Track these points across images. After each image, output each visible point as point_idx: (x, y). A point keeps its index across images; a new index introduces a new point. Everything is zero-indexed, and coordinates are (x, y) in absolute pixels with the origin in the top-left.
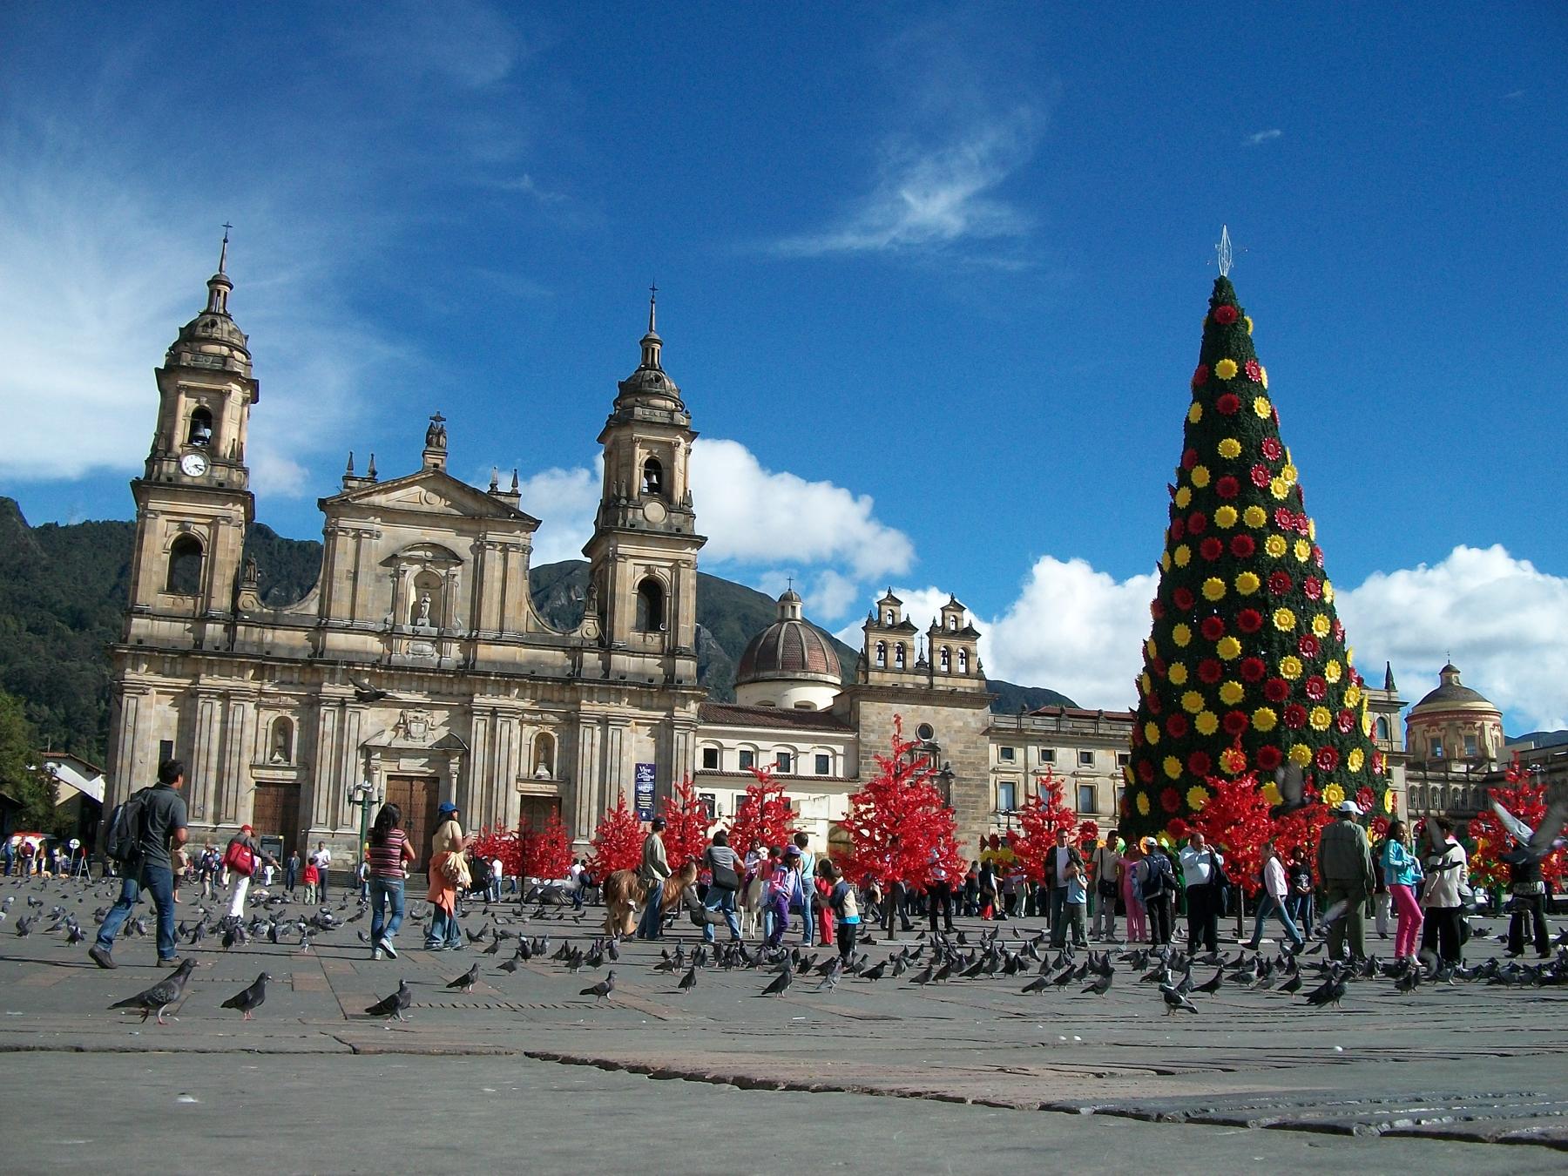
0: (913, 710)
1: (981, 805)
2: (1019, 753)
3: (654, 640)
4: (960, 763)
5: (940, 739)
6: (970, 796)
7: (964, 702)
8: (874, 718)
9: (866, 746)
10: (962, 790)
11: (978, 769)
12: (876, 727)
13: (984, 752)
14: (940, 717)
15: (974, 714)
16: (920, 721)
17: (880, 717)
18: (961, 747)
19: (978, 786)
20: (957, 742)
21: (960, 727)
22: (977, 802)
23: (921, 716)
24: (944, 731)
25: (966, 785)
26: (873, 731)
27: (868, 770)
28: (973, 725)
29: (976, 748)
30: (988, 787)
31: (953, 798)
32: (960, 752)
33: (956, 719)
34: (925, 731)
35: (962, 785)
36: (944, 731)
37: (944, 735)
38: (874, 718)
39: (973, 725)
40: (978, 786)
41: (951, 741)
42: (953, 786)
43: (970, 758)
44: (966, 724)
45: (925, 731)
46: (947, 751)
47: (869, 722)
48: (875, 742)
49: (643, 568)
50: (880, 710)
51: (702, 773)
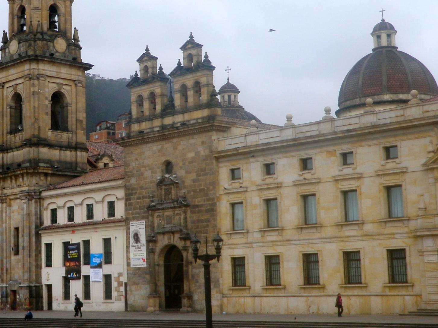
0: (159, 151)
1: (210, 229)
2: (245, 175)
3: (18, 138)
4: (194, 191)
5: (179, 172)
6: (202, 221)
7: (194, 134)
8: (133, 164)
10: (195, 217)
11: (207, 195)
12: (135, 172)
15: (203, 143)
16: (163, 159)
17: (137, 163)
18: (193, 176)
19: (207, 211)
20: (190, 173)
22: (207, 226)
24: (181, 164)
25: (199, 211)
26: (133, 176)
28: (202, 153)
29: (206, 174)
30: (215, 211)
31: (190, 225)
32: (194, 181)
34: (168, 166)
37: (181, 168)
39: (202, 153)
40: (207, 211)
42: (189, 214)
43: (200, 185)
44: (197, 153)
45: (168, 166)
46: (183, 182)
49: (55, 85)
51: (46, 229)
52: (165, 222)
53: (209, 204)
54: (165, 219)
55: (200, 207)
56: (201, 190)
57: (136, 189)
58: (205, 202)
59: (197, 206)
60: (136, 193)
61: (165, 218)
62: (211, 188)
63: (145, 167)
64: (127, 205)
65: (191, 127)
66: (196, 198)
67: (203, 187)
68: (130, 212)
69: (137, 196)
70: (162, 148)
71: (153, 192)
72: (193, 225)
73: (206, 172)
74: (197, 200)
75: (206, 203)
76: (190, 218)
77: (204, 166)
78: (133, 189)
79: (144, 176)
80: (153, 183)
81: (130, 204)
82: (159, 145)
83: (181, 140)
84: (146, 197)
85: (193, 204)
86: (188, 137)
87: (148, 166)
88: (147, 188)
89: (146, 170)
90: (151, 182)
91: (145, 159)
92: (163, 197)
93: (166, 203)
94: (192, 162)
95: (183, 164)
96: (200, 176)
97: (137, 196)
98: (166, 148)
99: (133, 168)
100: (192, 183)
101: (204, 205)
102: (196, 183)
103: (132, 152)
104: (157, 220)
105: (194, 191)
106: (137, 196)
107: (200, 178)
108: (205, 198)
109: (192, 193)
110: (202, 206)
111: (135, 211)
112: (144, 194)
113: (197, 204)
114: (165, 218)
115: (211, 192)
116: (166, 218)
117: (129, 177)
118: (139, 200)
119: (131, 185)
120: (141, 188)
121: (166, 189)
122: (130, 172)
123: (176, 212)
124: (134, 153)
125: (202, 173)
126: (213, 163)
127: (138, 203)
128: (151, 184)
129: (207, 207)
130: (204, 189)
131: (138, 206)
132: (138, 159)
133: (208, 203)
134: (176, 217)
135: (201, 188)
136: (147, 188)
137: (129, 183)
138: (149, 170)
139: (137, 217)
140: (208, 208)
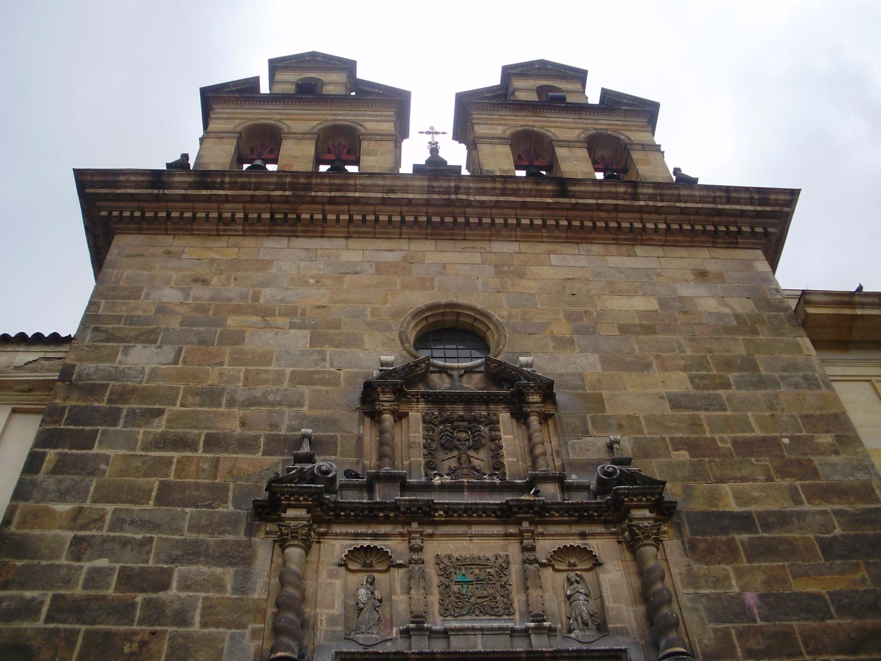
4: (692, 446)
9: (93, 390)
13: (810, 396)
14: (529, 285)
17: (197, 291)
21: (646, 314)
23: (423, 284)
24: (563, 329)
25: (757, 551)
26: (149, 338)
27: (62, 497)
29: (761, 383)
32: (676, 402)
33: (614, 290)
35: (730, 553)
36: (563, 329)
37: (563, 343)
38: (170, 295)
41: (608, 361)
47: (143, 307)
48: (154, 374)
50: (203, 270)
52: (435, 598)
53: (838, 513)
54: (435, 580)
55: (767, 527)
56: (745, 448)
57: (148, 395)
58: (800, 502)
59: (744, 521)
60: (160, 412)
61: (431, 570)
62: (825, 439)
63: (265, 313)
64: (47, 465)
65: (652, 197)
66: (722, 481)
67: (758, 433)
68: (62, 508)
69: (159, 430)
70: (409, 260)
71: (315, 422)
72: (733, 628)
73: (763, 372)
74: (727, 488)
75: (807, 507)
76: (692, 579)
77: (741, 350)
78: (123, 395)
79: (246, 347)
80: (323, 382)
81: (88, 466)
82: (390, 251)
83: (549, 253)
84: (246, 445)
85: (699, 505)
86: (596, 248)
87: (290, 312)
88: (253, 402)
89: (268, 326)
90: (307, 379)
91: (267, 284)
92: (419, 458)
93: (443, 488)
94: (648, 330)
95: (576, 331)
96: (726, 385)
97: (159, 426)
98: (444, 266)
99: (162, 309)
100: (669, 412)
101: (801, 515)
102: (702, 414)
103: (168, 253)
104: (338, 583)
105: (692, 446)
106: (159, 426)
107: (720, 392)
108: (798, 483)
109: (683, 455)
110: (782, 519)
111: (110, 508)
112: (232, 427)
113: (734, 507)
114: (431, 570)
115: (834, 459)
116: (445, 573)
117: (111, 337)
118: (176, 455)
119: (118, 375)
120: (212, 396)
121: (427, 421)
122: (131, 320)
123: (545, 546)
124: (184, 256)
125: (732, 376)
126: (798, 348)
127: (157, 467)
128: (306, 390)
129: (827, 527)
130: (769, 445)
131: (155, 483)
132: (215, 280)
133: (827, 507)
134: (548, 572)
135: (748, 435)
136: (253, 402)
137: (102, 365)
138: (293, 326)
139: (125, 543)
140: (838, 531)
